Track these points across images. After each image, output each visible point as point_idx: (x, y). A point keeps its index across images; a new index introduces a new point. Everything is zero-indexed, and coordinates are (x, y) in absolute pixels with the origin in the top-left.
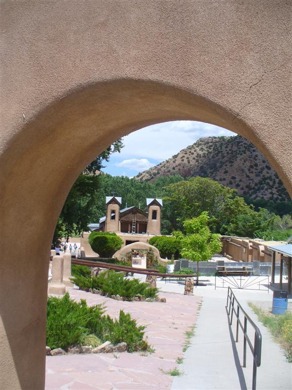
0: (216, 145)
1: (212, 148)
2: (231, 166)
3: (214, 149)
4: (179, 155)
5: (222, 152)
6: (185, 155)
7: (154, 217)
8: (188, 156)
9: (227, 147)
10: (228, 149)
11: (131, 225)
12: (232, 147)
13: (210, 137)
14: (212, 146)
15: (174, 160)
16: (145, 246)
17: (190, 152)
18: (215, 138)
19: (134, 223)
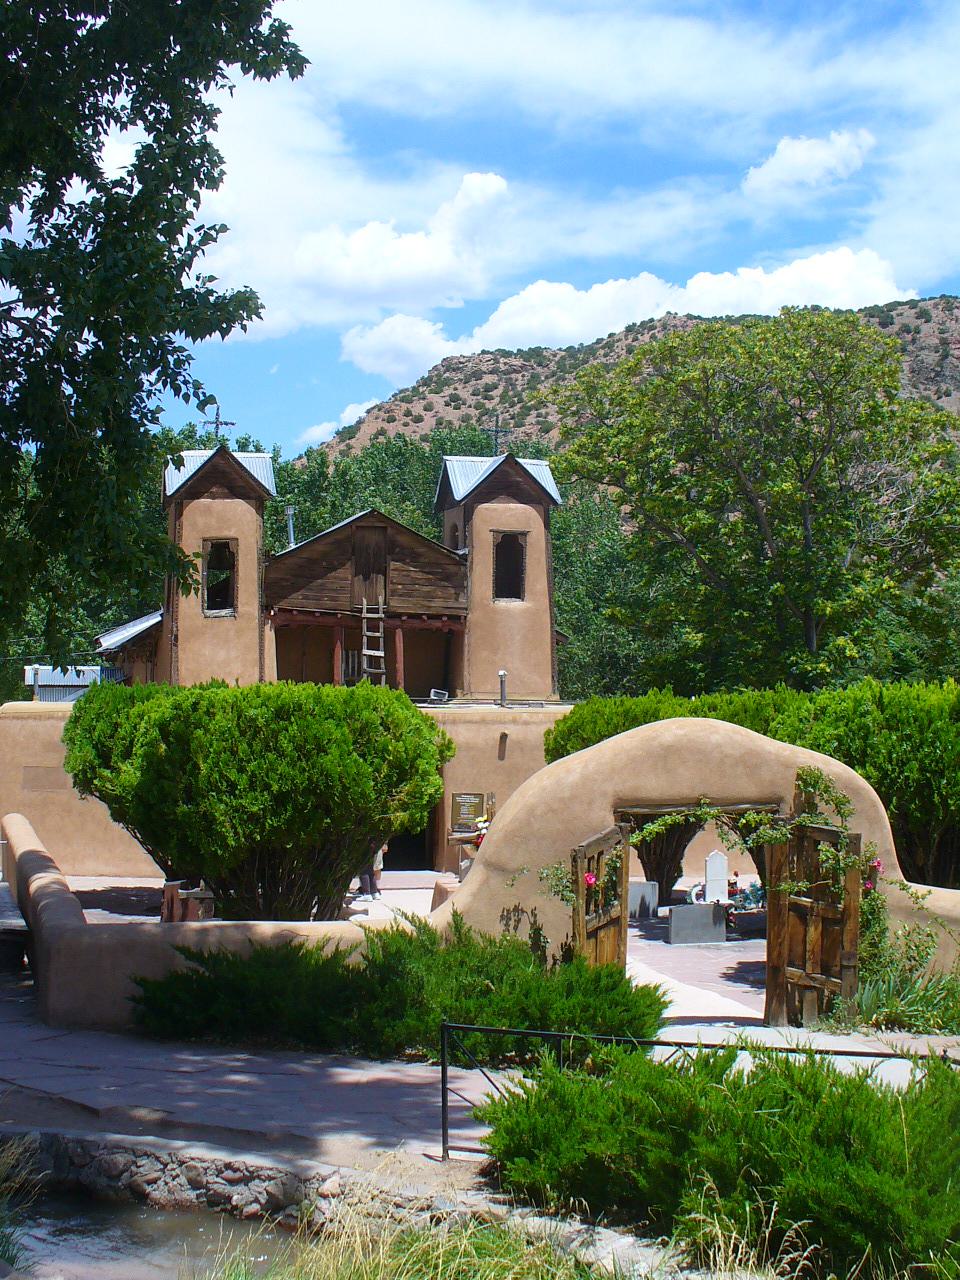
0: (511, 384)
3: (503, 398)
4: (364, 427)
6: (386, 425)
7: (509, 583)
8: (401, 430)
11: (353, 646)
13: (484, 352)
15: (342, 447)
16: (751, 761)
17: (408, 413)
18: (506, 354)
19: (373, 625)
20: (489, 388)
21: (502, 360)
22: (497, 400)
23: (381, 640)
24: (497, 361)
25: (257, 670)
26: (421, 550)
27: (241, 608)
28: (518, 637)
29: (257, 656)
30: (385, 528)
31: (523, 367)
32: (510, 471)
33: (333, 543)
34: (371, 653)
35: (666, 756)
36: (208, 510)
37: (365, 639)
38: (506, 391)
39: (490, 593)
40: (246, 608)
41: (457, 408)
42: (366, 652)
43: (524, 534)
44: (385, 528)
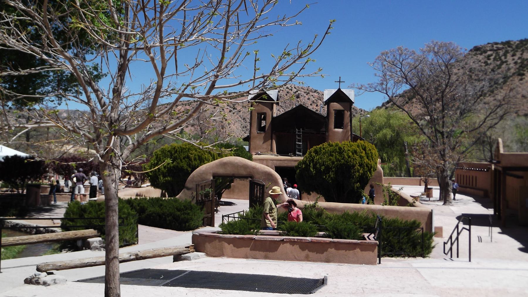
0: (497, 54)
1: (492, 57)
2: (521, 80)
3: (495, 59)
5: (506, 62)
9: (513, 55)
10: (516, 58)
12: (522, 54)
13: (489, 44)
14: (492, 55)
18: (496, 44)
20: (489, 56)
21: (495, 46)
22: (492, 60)
24: (493, 46)
31: (503, 48)
34: (300, 143)
35: (224, 164)
38: (495, 57)
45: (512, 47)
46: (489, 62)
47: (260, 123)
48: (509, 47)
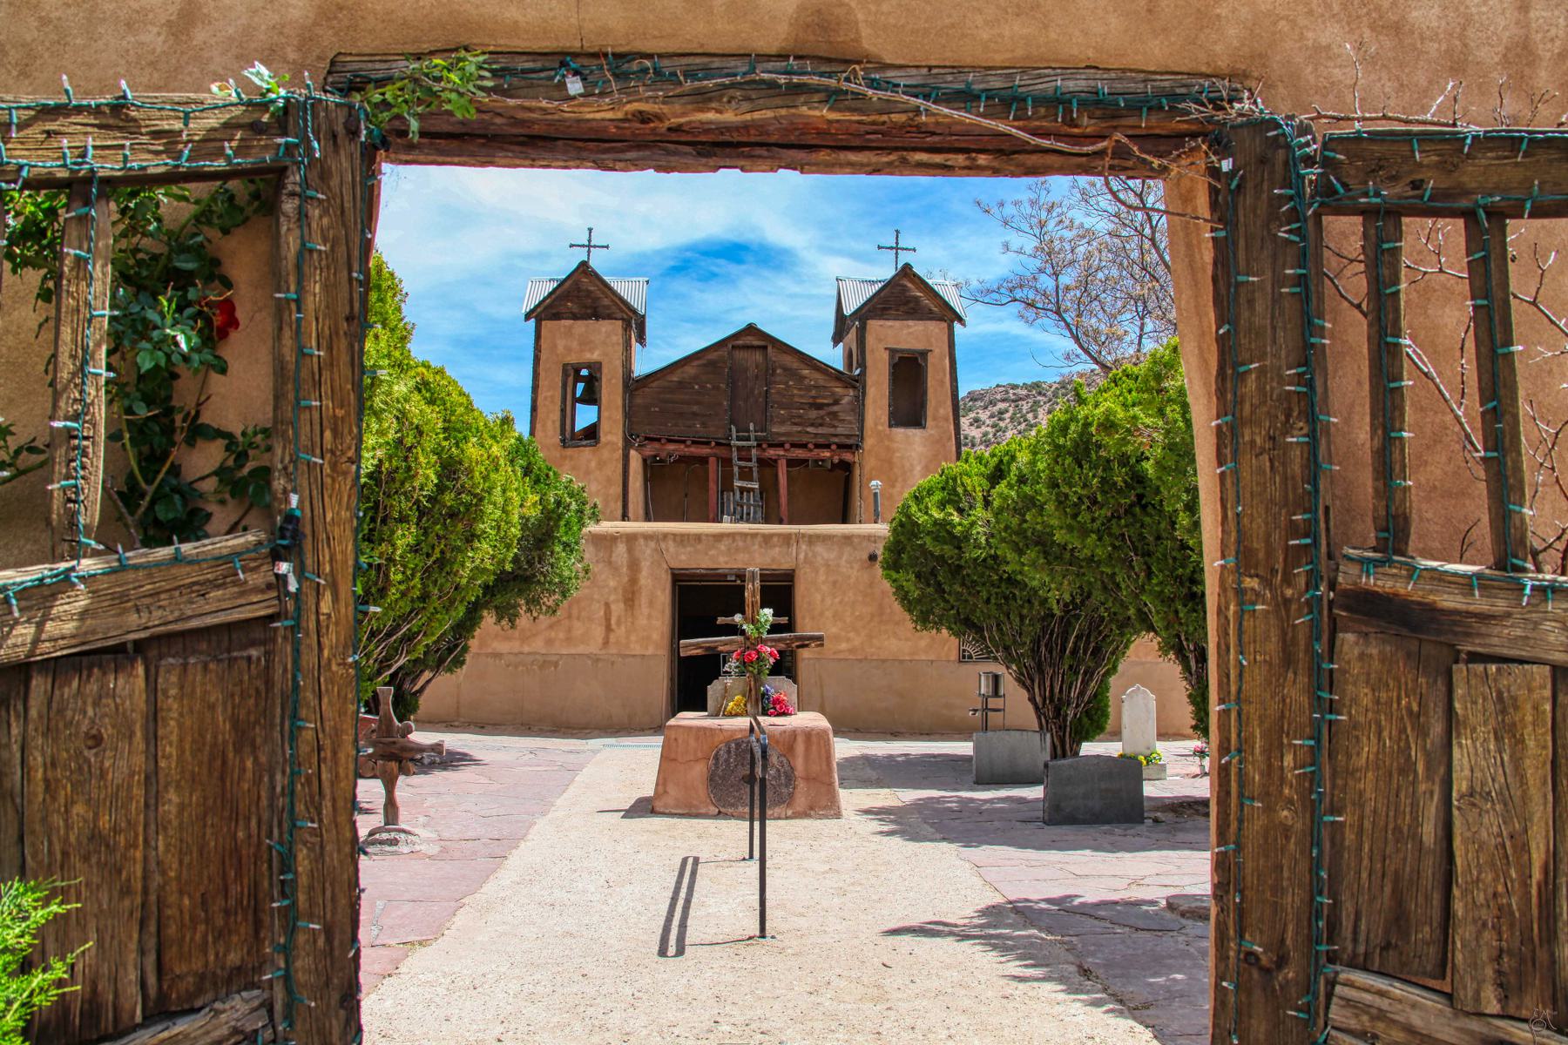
1: (1007, 416)
3: (1012, 419)
7: (908, 410)
13: (998, 386)
18: (1014, 387)
20: (1001, 412)
23: (755, 469)
24: (1007, 392)
25: (620, 504)
26: (806, 372)
27: (603, 439)
28: (919, 468)
29: (620, 490)
30: (765, 348)
32: (909, 285)
33: (704, 365)
36: (569, 333)
37: (736, 469)
39: (885, 418)
40: (609, 438)
41: (978, 427)
42: (737, 483)
43: (924, 354)
44: (765, 348)
45: (1044, 395)
46: (1002, 424)
47: (567, 416)
48: (1040, 393)
